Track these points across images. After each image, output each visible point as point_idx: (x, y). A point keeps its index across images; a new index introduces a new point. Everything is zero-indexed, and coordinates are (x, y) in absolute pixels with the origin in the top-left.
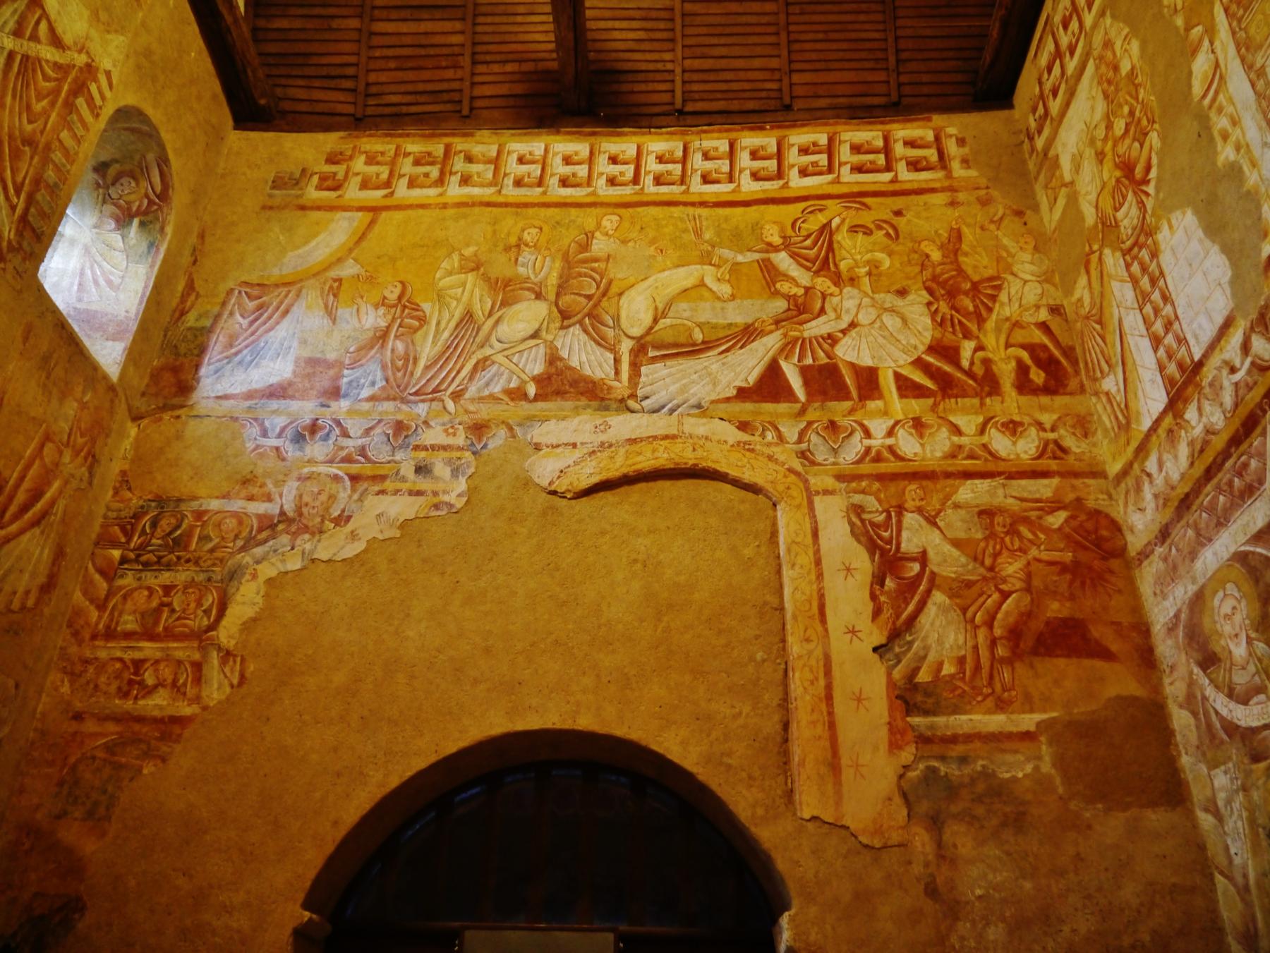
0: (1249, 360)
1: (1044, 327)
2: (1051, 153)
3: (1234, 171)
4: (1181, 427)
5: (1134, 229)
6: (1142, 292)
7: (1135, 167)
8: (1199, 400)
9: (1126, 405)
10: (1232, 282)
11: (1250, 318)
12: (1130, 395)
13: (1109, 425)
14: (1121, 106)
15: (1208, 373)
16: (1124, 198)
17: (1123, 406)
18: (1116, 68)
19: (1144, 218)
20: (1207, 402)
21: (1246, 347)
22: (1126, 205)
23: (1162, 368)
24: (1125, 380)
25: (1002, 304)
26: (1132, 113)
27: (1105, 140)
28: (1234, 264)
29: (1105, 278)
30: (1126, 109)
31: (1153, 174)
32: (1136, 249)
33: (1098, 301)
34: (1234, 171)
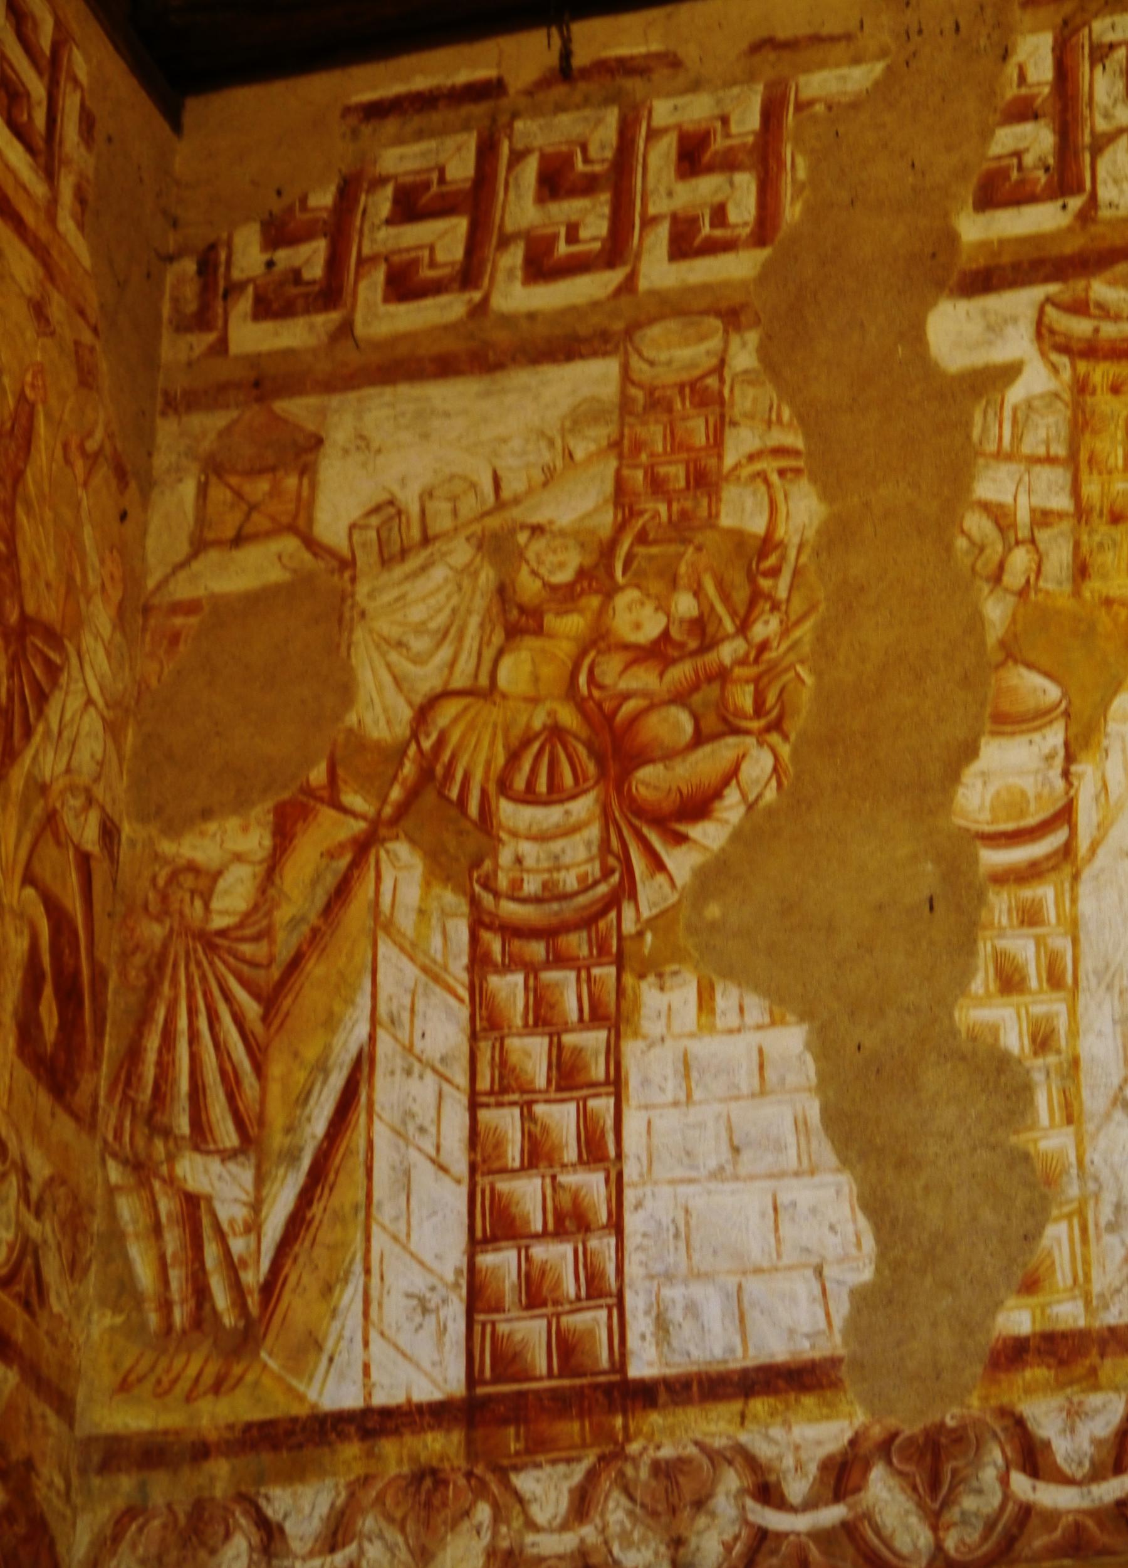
0: (832, 1514)
1: (84, 860)
2: (296, 408)
3: (1001, 1083)
4: (481, 1490)
5: (550, 894)
6: (502, 1064)
7: (643, 758)
8: (592, 1476)
9: (270, 1288)
10: (861, 1298)
11: (892, 1422)
12: (302, 1277)
13: (145, 1274)
14: (674, 584)
15: (666, 1435)
16: (556, 795)
17: (252, 1278)
18: (704, 481)
19: (613, 902)
20: (616, 1494)
21: (841, 1475)
22: (553, 815)
23: (478, 1296)
24: (297, 1223)
25: (47, 732)
26: (702, 629)
27: (566, 596)
28: (888, 1257)
29: (356, 912)
30: (685, 605)
31: (711, 835)
32: (537, 950)
33: (285, 945)
34: (1001, 1083)
